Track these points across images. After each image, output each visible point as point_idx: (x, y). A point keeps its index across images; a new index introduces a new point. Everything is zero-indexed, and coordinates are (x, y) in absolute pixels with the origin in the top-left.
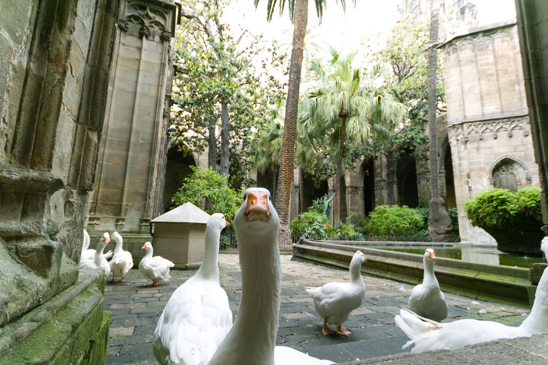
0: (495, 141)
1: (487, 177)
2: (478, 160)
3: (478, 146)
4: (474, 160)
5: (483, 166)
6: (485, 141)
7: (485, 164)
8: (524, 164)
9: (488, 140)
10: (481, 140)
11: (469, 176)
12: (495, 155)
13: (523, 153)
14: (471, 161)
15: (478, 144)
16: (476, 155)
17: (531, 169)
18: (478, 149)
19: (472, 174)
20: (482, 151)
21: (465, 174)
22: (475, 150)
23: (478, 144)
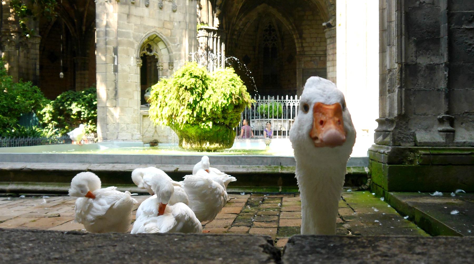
0: (146, 10)
1: (135, 55)
2: (128, 31)
3: (129, 12)
4: (124, 30)
5: (132, 39)
6: (136, 6)
7: (134, 38)
8: (169, 45)
9: (139, 7)
10: (133, 3)
11: (115, 51)
12: (146, 28)
13: (169, 31)
14: (121, 30)
15: (129, 8)
16: (126, 23)
17: (174, 53)
18: (128, 15)
19: (120, 48)
20: (133, 19)
21: (111, 47)
22: (126, 16)
23: (129, 8)
